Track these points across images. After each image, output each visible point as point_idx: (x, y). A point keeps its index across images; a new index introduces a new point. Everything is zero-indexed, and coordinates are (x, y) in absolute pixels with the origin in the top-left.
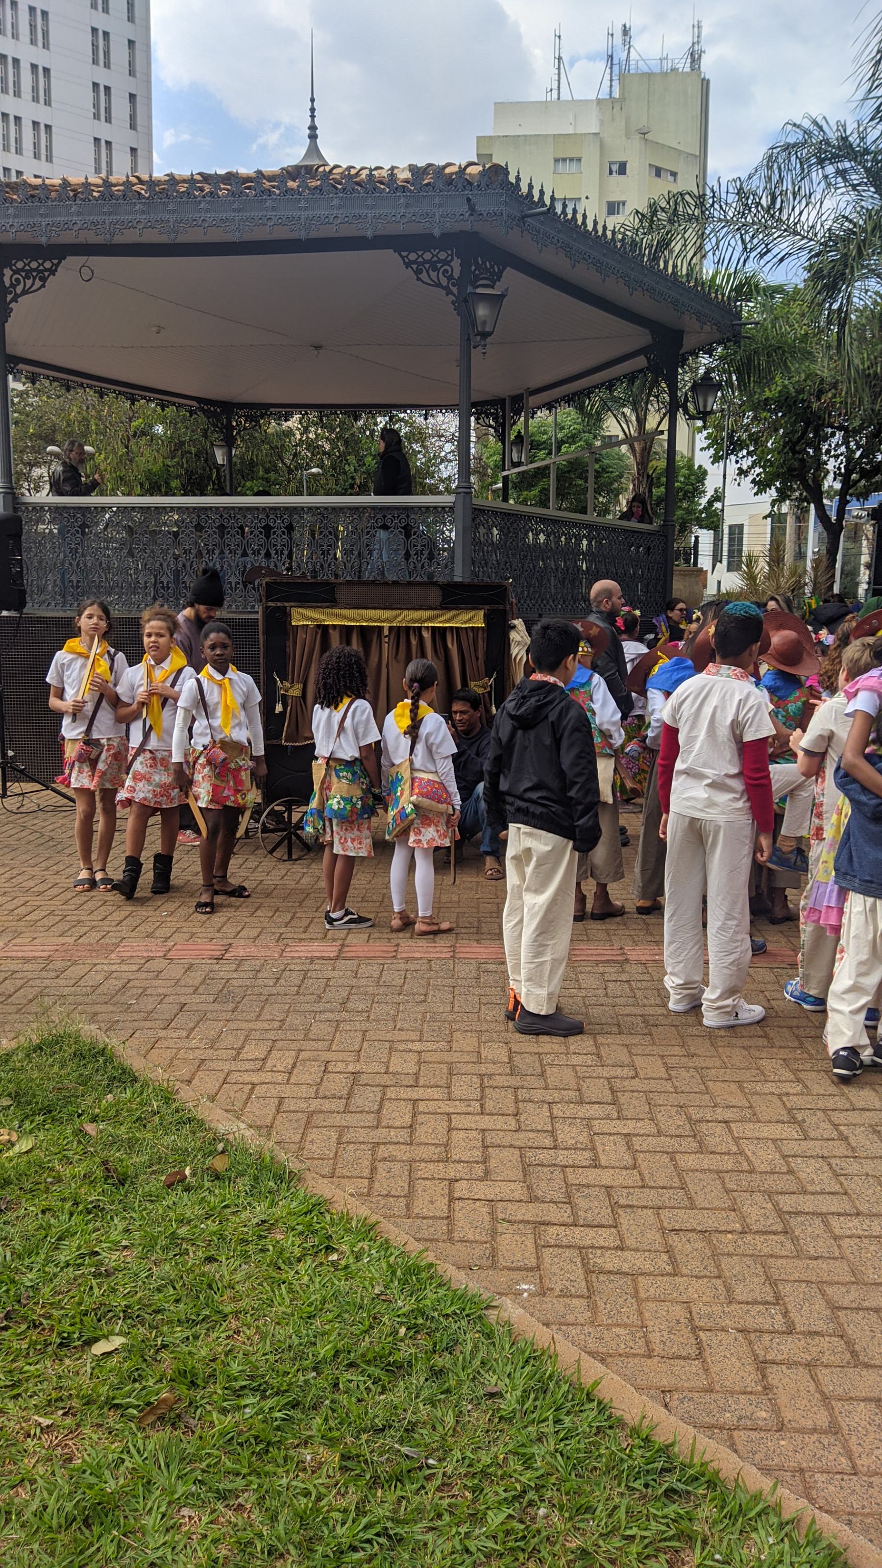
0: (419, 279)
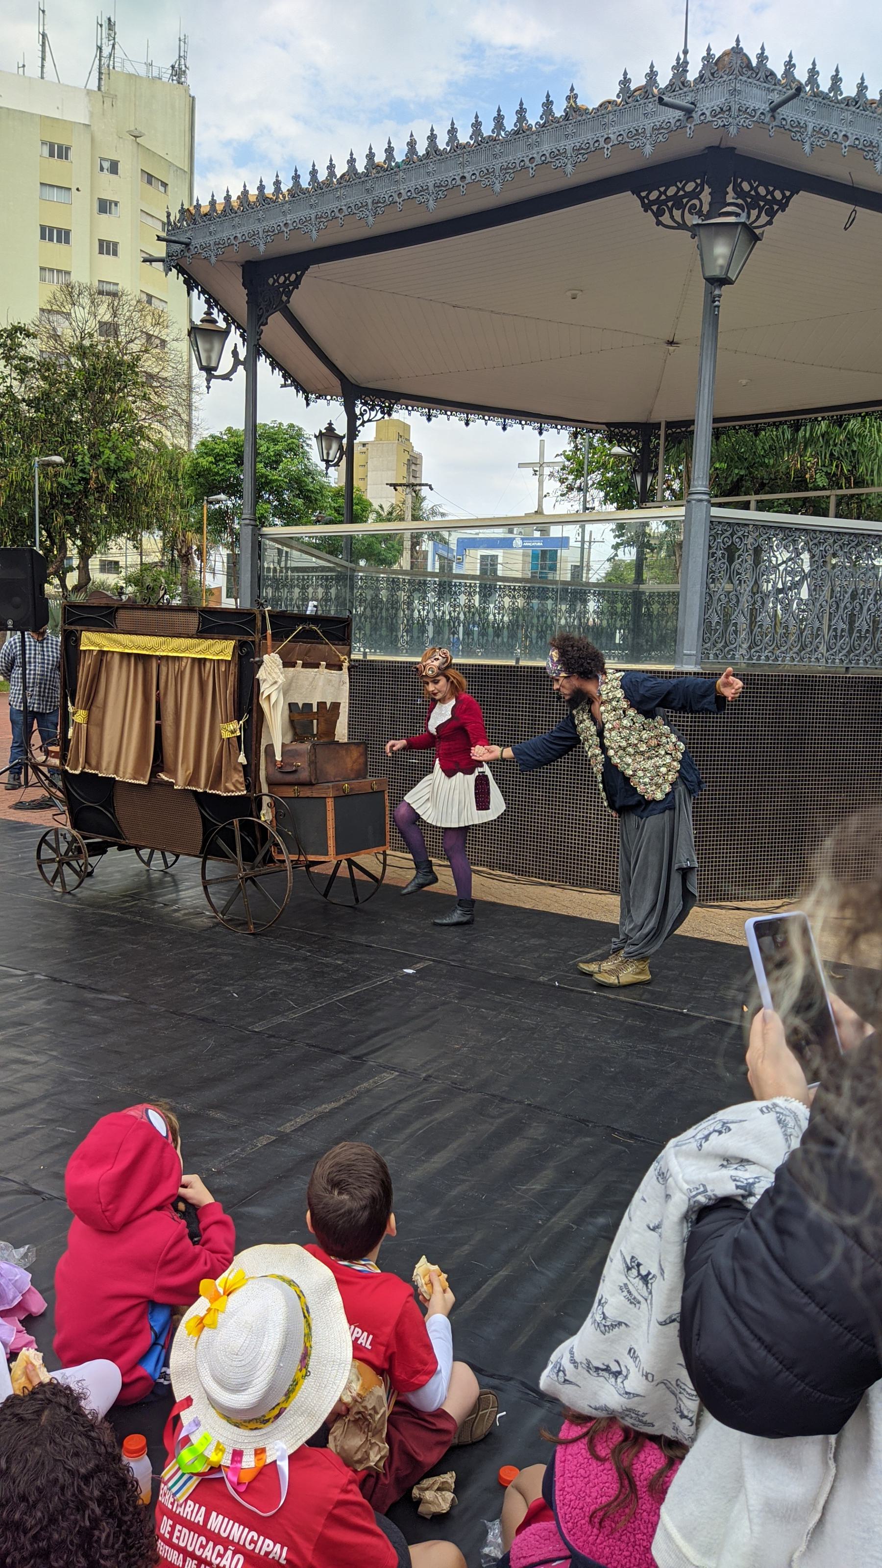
0: (659, 223)
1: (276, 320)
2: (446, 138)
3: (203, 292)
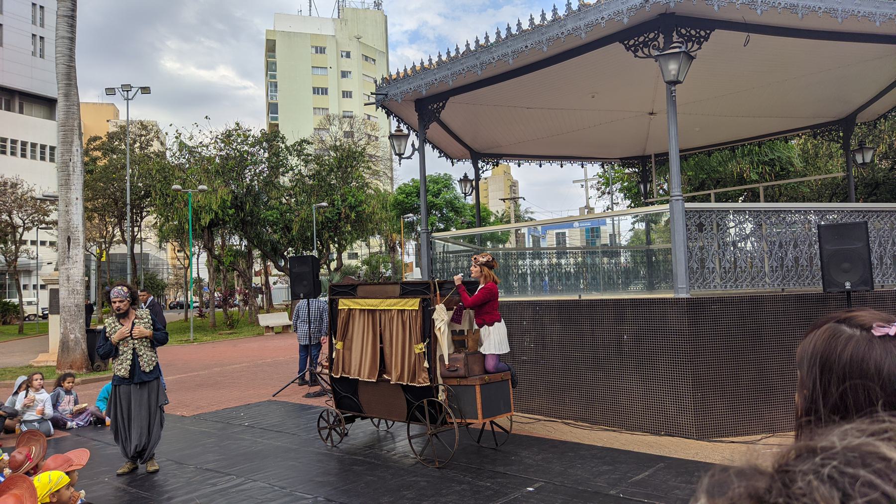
0: (636, 56)
1: (434, 127)
2: (516, 28)
3: (396, 116)
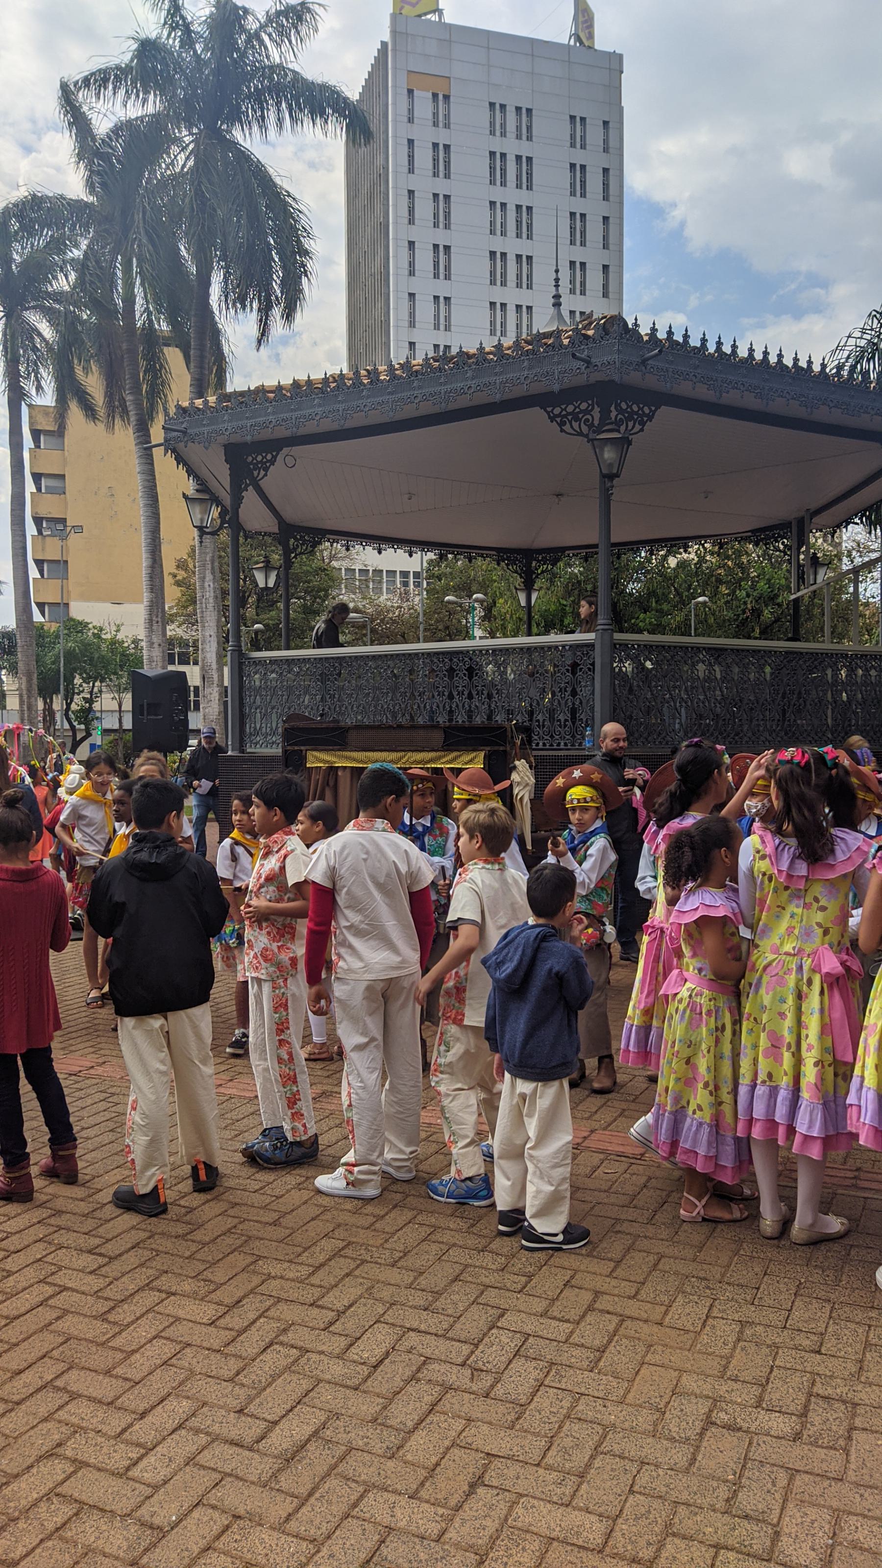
0: (562, 431)
